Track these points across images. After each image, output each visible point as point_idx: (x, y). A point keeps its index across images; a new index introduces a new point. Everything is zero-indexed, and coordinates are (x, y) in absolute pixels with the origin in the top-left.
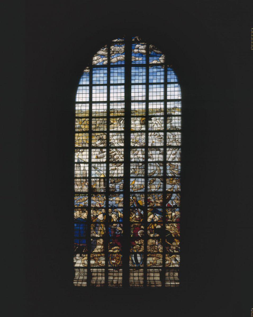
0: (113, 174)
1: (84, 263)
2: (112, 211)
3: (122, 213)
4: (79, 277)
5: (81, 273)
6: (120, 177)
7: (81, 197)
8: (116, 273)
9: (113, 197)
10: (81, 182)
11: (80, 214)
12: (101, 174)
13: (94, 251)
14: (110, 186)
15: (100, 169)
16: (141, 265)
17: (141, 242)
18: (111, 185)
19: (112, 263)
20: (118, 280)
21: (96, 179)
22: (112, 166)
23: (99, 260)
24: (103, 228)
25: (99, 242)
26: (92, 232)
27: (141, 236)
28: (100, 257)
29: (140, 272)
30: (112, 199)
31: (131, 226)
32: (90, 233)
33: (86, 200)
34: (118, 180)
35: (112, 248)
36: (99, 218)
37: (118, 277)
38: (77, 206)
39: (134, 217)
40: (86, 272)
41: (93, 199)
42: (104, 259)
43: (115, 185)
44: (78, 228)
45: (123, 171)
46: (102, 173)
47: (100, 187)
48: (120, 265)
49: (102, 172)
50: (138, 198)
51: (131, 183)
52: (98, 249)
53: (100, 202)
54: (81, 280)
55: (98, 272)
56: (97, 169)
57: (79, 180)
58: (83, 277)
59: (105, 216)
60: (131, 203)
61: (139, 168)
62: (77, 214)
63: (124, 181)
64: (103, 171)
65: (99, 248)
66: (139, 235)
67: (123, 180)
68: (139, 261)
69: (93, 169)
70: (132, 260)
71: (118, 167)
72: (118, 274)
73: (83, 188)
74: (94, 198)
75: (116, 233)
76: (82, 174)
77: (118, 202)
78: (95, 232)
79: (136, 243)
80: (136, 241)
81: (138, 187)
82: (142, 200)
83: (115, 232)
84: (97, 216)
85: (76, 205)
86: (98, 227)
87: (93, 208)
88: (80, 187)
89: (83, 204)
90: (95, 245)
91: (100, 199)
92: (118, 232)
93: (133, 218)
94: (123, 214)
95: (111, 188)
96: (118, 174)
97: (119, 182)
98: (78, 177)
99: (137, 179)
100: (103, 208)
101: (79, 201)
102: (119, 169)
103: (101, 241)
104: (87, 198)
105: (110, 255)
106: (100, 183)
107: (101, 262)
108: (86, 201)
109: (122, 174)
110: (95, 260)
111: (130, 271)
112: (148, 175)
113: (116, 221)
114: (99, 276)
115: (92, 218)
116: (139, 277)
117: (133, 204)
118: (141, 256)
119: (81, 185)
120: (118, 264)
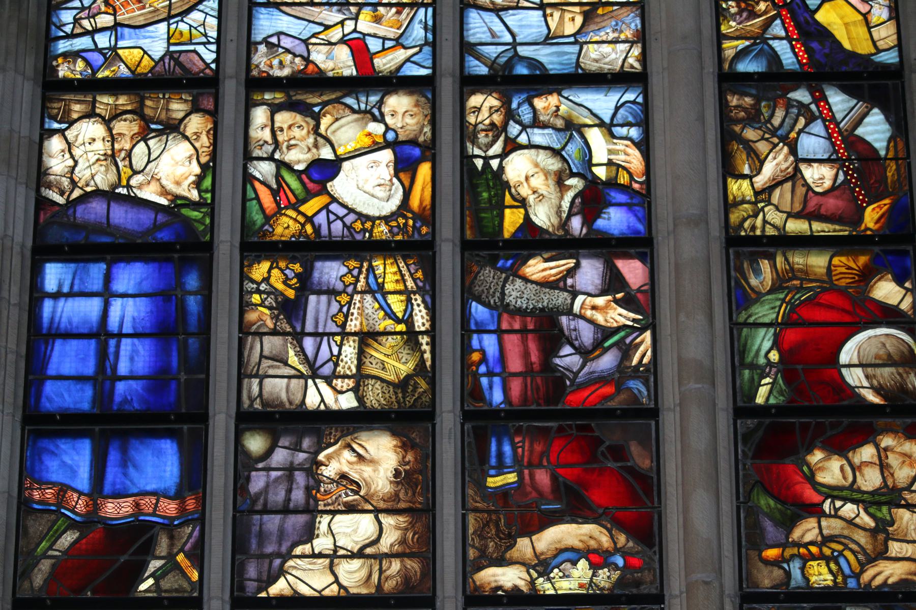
2: (510, 115)
3: (634, 132)
11: (112, 157)
17: (883, 467)
24: (397, 304)
25: (343, 476)
27: (877, 390)
31: (754, 281)
35: (523, 546)
38: (80, 65)
44: (91, 308)
52: (333, 557)
53: (365, 24)
60: (729, 27)
62: (77, 152)
65: (349, 543)
66: (855, 377)
75: (567, 358)
77: (579, 20)
79: (824, 478)
80: (817, 456)
86: (332, 292)
89: (158, 49)
90: (296, 512)
92: (586, 354)
93: (764, 194)
94: (637, 145)
103: (372, 462)
108: (196, 17)
113: (564, 224)
117: (760, 39)
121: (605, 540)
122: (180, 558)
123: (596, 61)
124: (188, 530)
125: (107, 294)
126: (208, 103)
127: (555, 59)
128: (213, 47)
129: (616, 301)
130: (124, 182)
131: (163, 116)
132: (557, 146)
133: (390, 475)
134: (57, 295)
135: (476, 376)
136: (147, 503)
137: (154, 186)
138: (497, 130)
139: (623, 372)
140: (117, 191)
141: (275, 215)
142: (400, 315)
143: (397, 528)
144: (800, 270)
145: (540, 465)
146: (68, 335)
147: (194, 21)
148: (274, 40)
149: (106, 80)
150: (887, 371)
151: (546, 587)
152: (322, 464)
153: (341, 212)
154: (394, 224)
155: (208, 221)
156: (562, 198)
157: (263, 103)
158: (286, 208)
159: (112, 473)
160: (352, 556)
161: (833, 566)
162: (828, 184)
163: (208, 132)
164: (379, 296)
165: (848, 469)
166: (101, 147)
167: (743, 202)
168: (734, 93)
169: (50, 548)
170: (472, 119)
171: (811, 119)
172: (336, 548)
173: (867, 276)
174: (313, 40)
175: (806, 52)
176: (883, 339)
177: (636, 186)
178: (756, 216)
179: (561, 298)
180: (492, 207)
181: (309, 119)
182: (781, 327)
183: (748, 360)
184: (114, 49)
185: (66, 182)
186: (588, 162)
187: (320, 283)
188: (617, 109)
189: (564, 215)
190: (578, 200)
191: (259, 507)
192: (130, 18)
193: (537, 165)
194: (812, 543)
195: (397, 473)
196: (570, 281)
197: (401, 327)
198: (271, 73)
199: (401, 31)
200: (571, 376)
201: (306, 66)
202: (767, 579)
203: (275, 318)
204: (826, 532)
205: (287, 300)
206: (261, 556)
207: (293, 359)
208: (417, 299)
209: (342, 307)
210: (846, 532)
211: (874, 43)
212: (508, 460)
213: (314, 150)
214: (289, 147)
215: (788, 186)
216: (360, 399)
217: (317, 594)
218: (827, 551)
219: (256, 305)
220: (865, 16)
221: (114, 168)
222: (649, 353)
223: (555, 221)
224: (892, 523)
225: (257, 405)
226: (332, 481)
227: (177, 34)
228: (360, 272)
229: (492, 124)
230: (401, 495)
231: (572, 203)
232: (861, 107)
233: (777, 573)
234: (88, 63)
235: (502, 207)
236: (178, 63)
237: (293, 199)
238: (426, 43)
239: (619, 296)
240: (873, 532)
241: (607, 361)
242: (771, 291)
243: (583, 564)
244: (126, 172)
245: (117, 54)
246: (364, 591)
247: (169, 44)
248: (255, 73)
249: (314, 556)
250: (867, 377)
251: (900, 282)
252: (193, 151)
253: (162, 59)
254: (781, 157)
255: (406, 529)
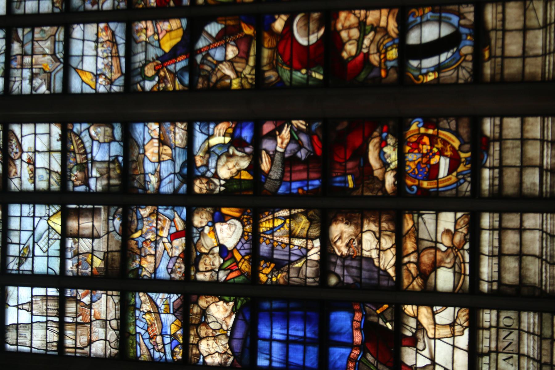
0: (50, 172)
1: (452, 325)
2: (203, 176)
3: (212, 126)
4: (528, 357)
5: (502, 345)
6: (64, 138)
7: (138, 330)
8: (507, 153)
9: (145, 174)
10: (77, 324)
11: (215, 337)
12: (50, 228)
13: (391, 272)
14: (96, 185)
15: (31, 233)
16: (462, 22)
17: (350, 28)
18: (92, 182)
19: (450, 172)
20: (542, 141)
21: (69, 254)
22: (20, 178)
23: (436, 242)
24: (278, 223)
25: (347, 245)
26: (295, 280)
27: (318, 30)
28: (418, 241)
29: (503, 25)
30: (153, 179)
31: (273, 79)
32: (303, 286)
33: (153, 302)
34: (74, 151)
35: (377, 173)
36: (235, 242)
37: (528, 139)
38: (177, 350)
39: (234, 70)
40: (498, 317)
41: (151, 270)
42: (429, 218)
43: (93, 161)
45: (42, 128)
46: (46, 226)
47: (99, 237)
48: (463, 131)
49: (42, 226)
50: (153, 52)
51: (88, 90)
52: (380, 250)
53: (164, 234)
54: (540, 348)
55: (496, 251)
56: (28, 247)
57: (69, 332)
58: (525, 336)
59: (225, 210)
60: (170, 86)
61: (30, 52)
62: (212, 351)
63: (81, 122)
64: (37, 220)
65: (374, 244)
66: (313, 39)
67: (77, 127)
68: (446, 31)
69: (27, 266)
70: (439, 68)
71: (22, 151)
72: (509, 144)
73: (103, 317)
74: (145, 264)
75: (302, 154)
76: (44, 319)
78: (296, 261)
81: (105, 55)
82: (158, 34)
83: (299, 159)
84: (222, 247)
85: (173, 353)
86: (273, 248)
87: (187, 272)
88: (99, 332)
89: (171, 318)
90: (361, 264)
91: (151, 236)
92: (301, 146)
93: (238, 74)
94: (217, 125)
95: (105, 182)
96: (50, 151)
97: (84, 147)
98: (56, 339)
99: (74, 62)
100: (188, 222)
101: (159, 339)
102: (33, 146)
103: (342, 233)
104: (143, 299)
105: (410, 187)
106: (83, 237)
107: (447, 231)
108: (159, 302)
109: (49, 134)
110: (435, 266)
111: (493, 76)
112: (57, 10)
113: (248, 155)
114: (521, 243)
115: (230, 276)
116: (529, 24)
117: (175, 75)
118: (421, 25)
119: (91, 322)
120: (456, 144)
121: (376, 140)
122: (378, 312)
123: (182, 141)
124: (367, 308)
125: (271, 340)
126: (194, 297)
127: (181, 158)
128: (172, 295)
129: (280, 133)
130: (225, 332)
131: (199, 316)
132: (216, 157)
133: (347, 226)
134: (271, 360)
135: (308, 191)
136: (356, 324)
137: (228, 320)
138: (209, 181)
139: (308, 132)
140: (229, 335)
141: (241, 271)
142: (283, 221)
143: (369, 224)
144: (270, 60)
145: (345, 166)
146: (287, 356)
147: (160, 303)
148: (170, 270)
149: (183, 339)
150: (312, 26)
151: (394, 164)
152: (342, 254)
153: (240, 244)
154: (246, 223)
155: (242, 298)
156: (237, 156)
157: (195, 275)
158: (238, 266)
159: (344, 339)
160: (379, 242)
161: (389, 49)
162: (235, 49)
163: (206, 298)
164: (275, 230)
165: (351, 42)
166: (211, 342)
167: (241, 83)
168: (197, 85)
169: (373, 365)
170: (204, 191)
171: (208, 54)
172: (376, 249)
173: (273, 33)
174: (170, 254)
175: (181, 56)
176: (299, 27)
177: (234, 126)
178: (246, 78)
179: (278, 157)
180: (240, 184)
181: (202, 257)
182: (293, 68)
183: (304, 81)
184: (171, 336)
185: (225, 356)
186: (223, 145)
187: (269, 253)
188: (202, 133)
189: (245, 155)
190: (239, 149)
191: (358, 279)
192: (159, 329)
193: (224, 165)
194: (380, 57)
195: (347, 223)
196: (271, 153)
197: (288, 221)
198: (183, 272)
199: (168, 219)
200: (309, 153)
201: (181, 258)
202: (393, 75)
203: (282, 272)
204: (375, 51)
205: (275, 267)
206: (379, 279)
207: (298, 265)
208: (277, 214)
209: (279, 245)
210: (376, 43)
211: (178, 28)
212: (343, 179)
213: (215, 255)
214: (213, 265)
215: (235, 64)
216: (316, 238)
217: (395, 257)
218: (383, 51)
219: (277, 279)
220: (167, 32)
221: (220, 336)
222: (301, 121)
223: (246, 158)
224: (372, 25)
225: (317, 279)
226: (349, 250)
227: (166, 310)
228: (265, 237)
229: (207, 183)
230: (355, 222)
231: (239, 151)
232: (204, 35)
233: (391, 71)
234: (176, 347)
235: (240, 180)
236: (177, 310)
237: (235, 264)
238: (173, 209)
239: (277, 133)
240: (376, 32)
241: (304, 139)
242: (277, 71)
243: (386, 150)
244: (221, 332)
245: (174, 334)
246: (394, 238)
247: (170, 313)
248: (183, 278)
249: (379, 258)
250: (313, 33)
251: (275, 20)
252: (214, 304)
253: (176, 316)
254: (224, 67)
255: (370, 221)
